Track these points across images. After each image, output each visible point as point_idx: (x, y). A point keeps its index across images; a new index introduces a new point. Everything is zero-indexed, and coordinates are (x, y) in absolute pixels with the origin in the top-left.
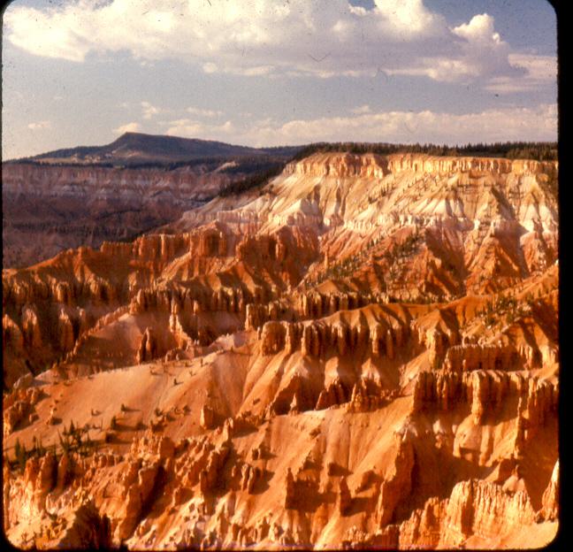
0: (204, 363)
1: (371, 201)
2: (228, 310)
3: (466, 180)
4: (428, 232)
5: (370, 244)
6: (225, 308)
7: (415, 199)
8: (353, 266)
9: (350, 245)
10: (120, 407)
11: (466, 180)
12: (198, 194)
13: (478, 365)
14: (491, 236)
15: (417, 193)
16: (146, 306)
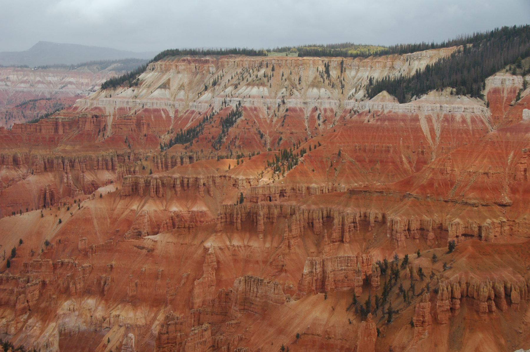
0: (81, 205)
1: (206, 88)
2: (107, 169)
3: (270, 73)
4: (245, 109)
5: (205, 120)
6: (105, 167)
7: (236, 87)
8: (194, 134)
9: (192, 120)
10: (18, 241)
11: (270, 73)
12: (94, 86)
13: (268, 198)
14: (287, 110)
15: (237, 82)
16: (45, 168)
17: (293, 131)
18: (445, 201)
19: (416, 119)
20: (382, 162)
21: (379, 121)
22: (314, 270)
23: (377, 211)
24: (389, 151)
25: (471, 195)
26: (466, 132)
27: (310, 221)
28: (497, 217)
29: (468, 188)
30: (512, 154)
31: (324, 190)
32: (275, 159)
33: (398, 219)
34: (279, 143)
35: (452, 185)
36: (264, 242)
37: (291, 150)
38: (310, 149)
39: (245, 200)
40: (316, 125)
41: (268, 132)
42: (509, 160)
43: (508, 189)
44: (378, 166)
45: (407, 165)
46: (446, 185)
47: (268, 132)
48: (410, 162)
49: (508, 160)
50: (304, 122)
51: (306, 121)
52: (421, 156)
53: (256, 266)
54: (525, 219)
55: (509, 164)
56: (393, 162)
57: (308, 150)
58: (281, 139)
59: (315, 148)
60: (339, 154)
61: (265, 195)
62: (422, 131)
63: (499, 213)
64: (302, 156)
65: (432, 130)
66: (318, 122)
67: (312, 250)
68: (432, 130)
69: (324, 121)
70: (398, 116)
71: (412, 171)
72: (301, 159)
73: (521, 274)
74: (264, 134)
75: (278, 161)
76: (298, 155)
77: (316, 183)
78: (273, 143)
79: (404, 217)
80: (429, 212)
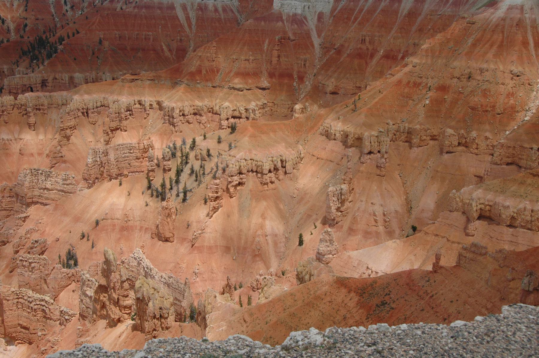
13: (30, 89)
17: (39, 17)
18: (214, 87)
19: (172, 7)
20: (143, 50)
21: (136, 8)
22: (98, 159)
23: (151, 99)
24: (149, 39)
25: (236, 81)
26: (219, 20)
27: (85, 111)
28: (259, 100)
29: (232, 74)
30: (267, 41)
31: (89, 79)
32: (30, 47)
33: (174, 105)
34: (24, 30)
35: (218, 72)
36: (37, 134)
37: (46, 37)
38: (68, 37)
39: (3, 91)
40: (64, 11)
41: (9, 16)
42: (266, 47)
43: (266, 74)
44: (140, 54)
45: (167, 53)
46: (213, 71)
47: (9, 16)
48: (170, 50)
49: (264, 47)
50: (50, 7)
51: (52, 6)
52: (179, 44)
53: (32, 158)
54: (282, 100)
55: (265, 51)
56: (154, 50)
57: (66, 38)
58: (26, 26)
59: (74, 36)
60: (100, 42)
61: (25, 85)
62: (178, 19)
63: (260, 96)
64: (61, 44)
65: (188, 19)
66: (65, 8)
67: (89, 140)
68: (188, 19)
69: (72, 7)
70: (154, 3)
71: (173, 59)
72: (60, 47)
73: (291, 148)
74: (5, 19)
75: (34, 48)
76: (56, 43)
77: (79, 72)
78: (17, 30)
79: (178, 103)
80: (201, 98)
